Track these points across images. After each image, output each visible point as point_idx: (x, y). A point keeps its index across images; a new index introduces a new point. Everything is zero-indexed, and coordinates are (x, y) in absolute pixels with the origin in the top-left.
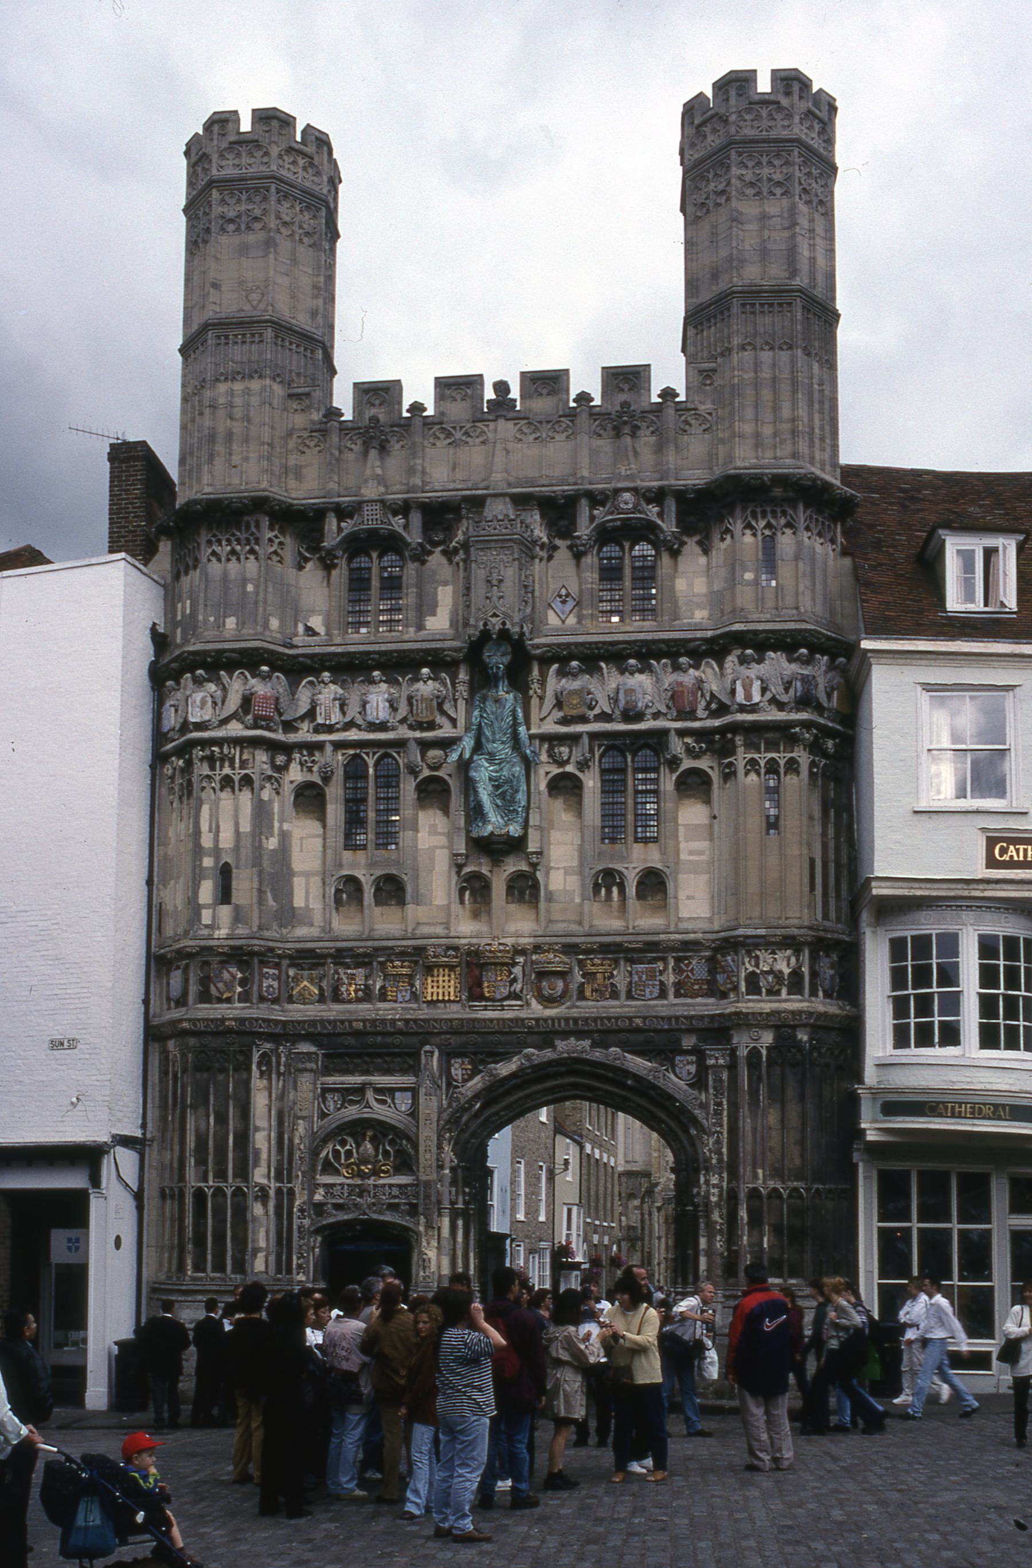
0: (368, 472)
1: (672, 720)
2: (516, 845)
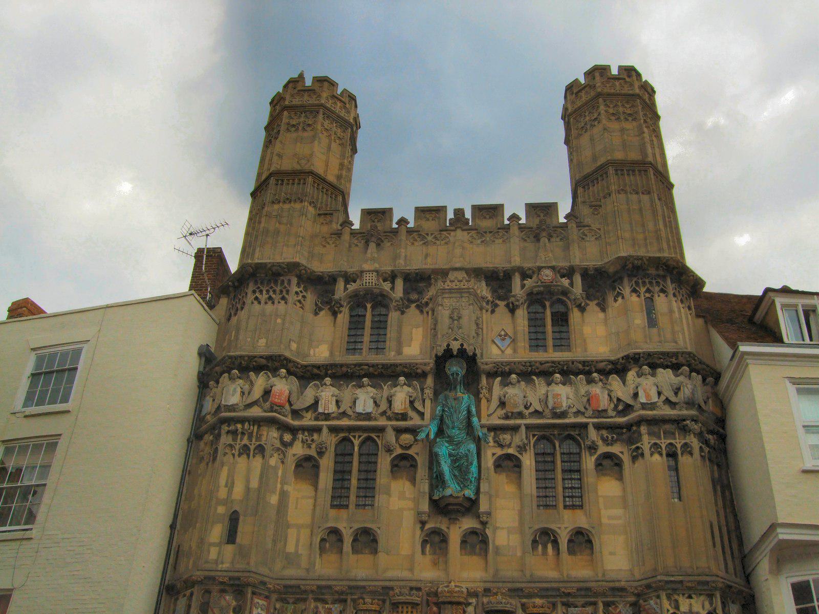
0: (369, 255)
1: (590, 417)
2: (470, 506)
